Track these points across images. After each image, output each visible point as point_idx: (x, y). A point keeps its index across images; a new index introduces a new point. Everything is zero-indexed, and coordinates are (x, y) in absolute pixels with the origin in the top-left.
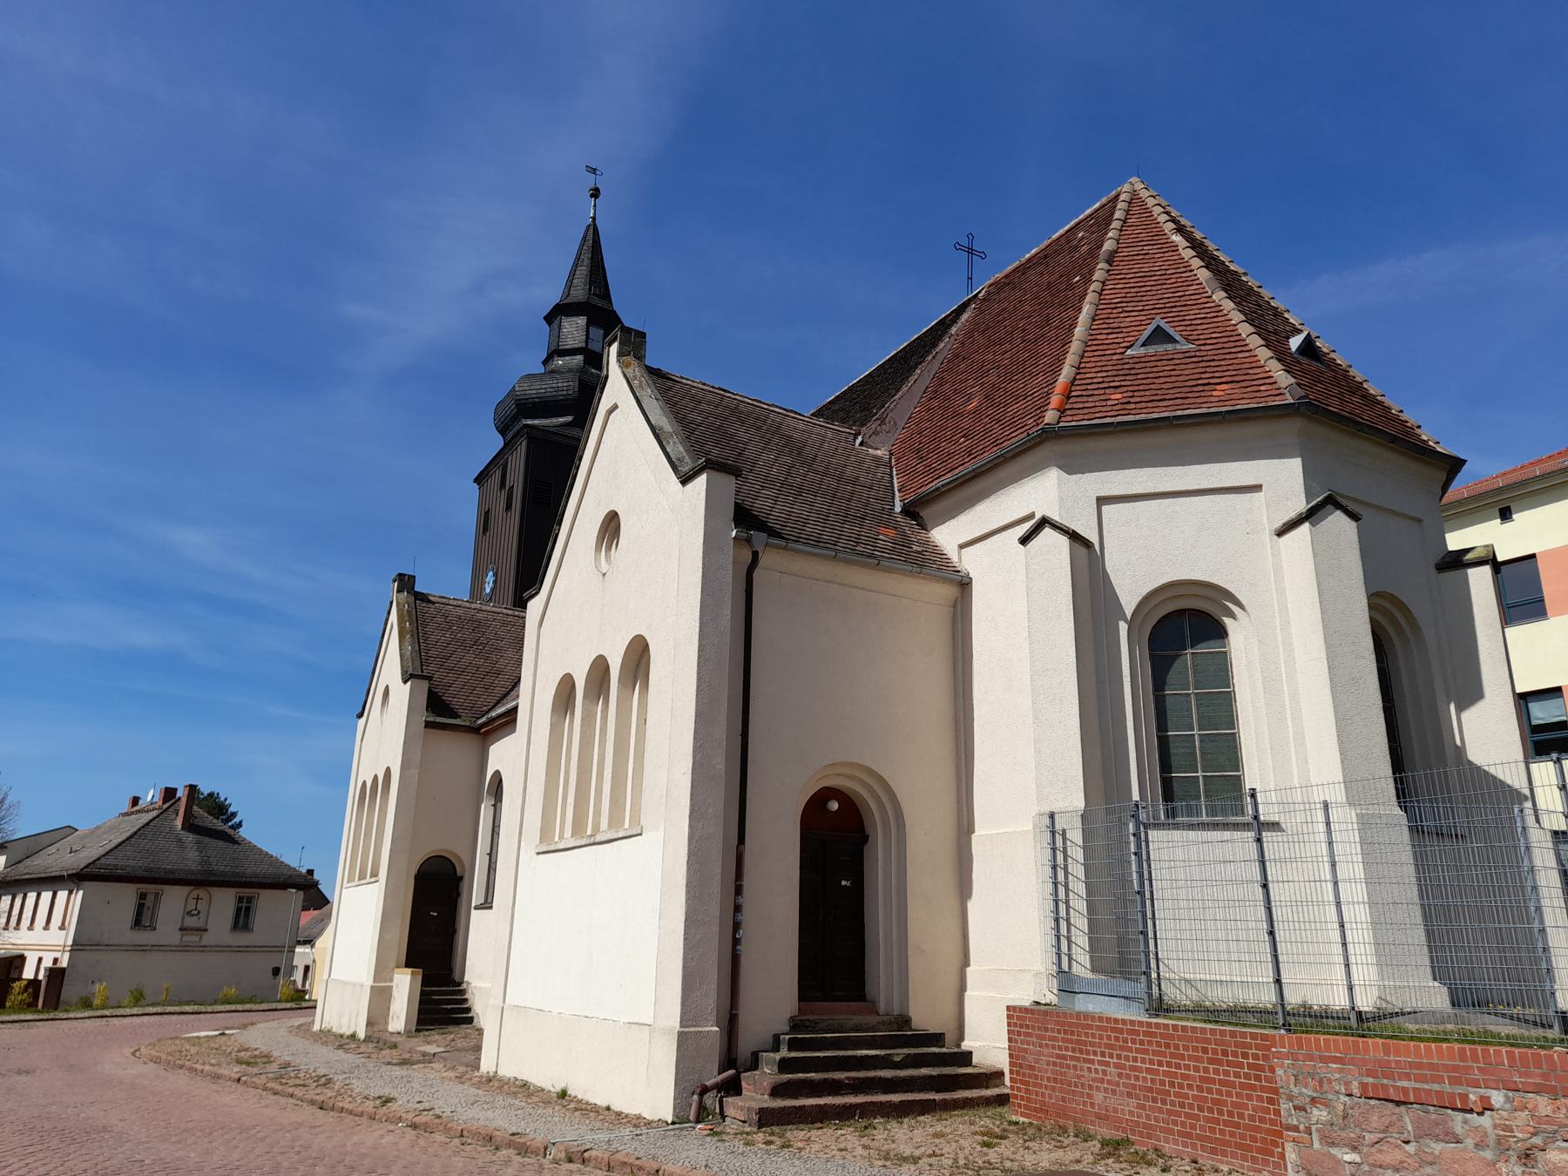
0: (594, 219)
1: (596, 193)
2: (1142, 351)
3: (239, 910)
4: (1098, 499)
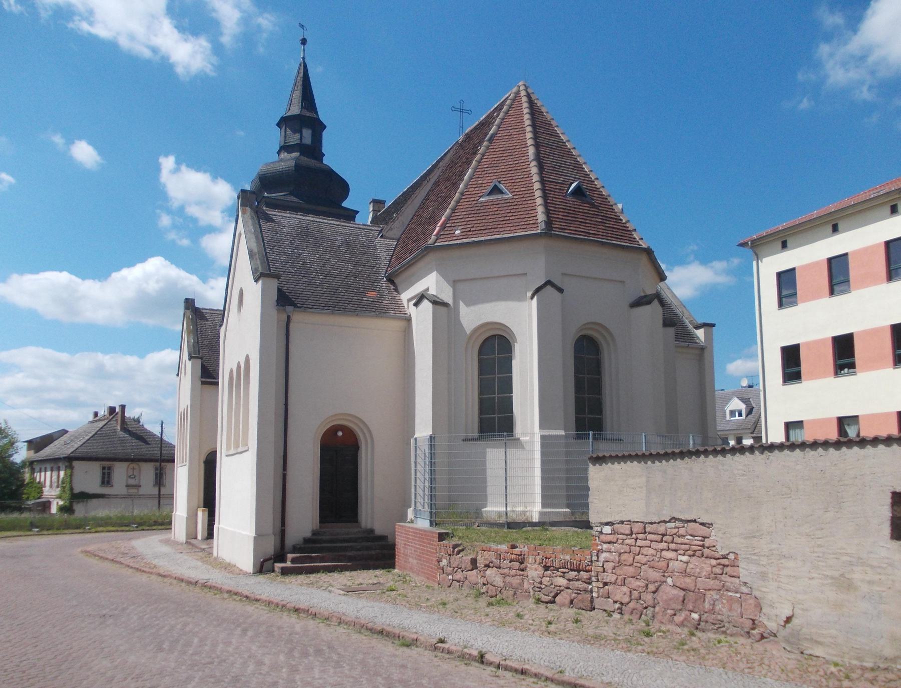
0: (304, 58)
1: (304, 42)
2: (487, 198)
3: (103, 474)
4: (454, 281)
